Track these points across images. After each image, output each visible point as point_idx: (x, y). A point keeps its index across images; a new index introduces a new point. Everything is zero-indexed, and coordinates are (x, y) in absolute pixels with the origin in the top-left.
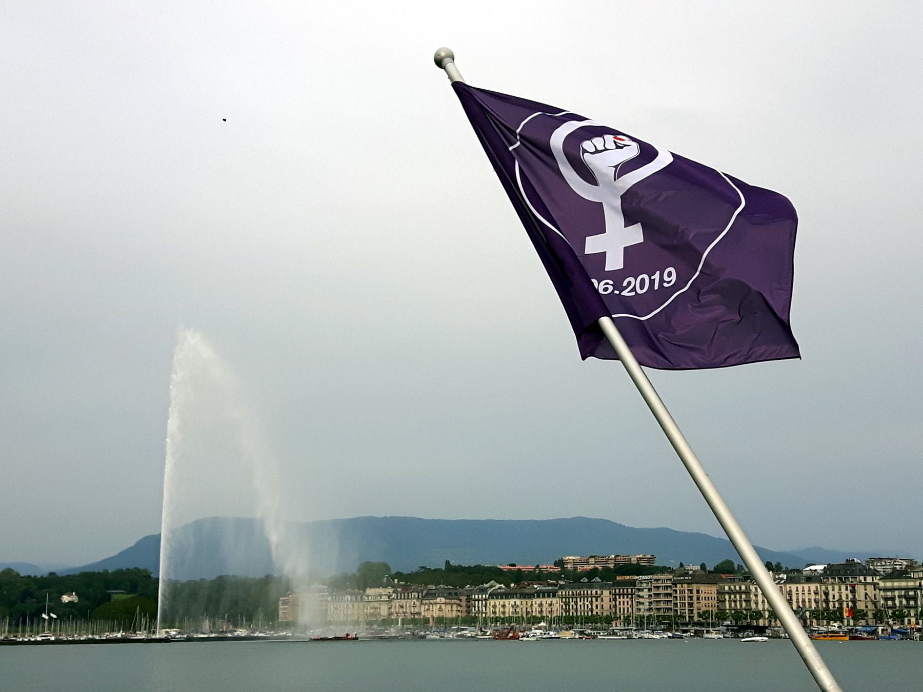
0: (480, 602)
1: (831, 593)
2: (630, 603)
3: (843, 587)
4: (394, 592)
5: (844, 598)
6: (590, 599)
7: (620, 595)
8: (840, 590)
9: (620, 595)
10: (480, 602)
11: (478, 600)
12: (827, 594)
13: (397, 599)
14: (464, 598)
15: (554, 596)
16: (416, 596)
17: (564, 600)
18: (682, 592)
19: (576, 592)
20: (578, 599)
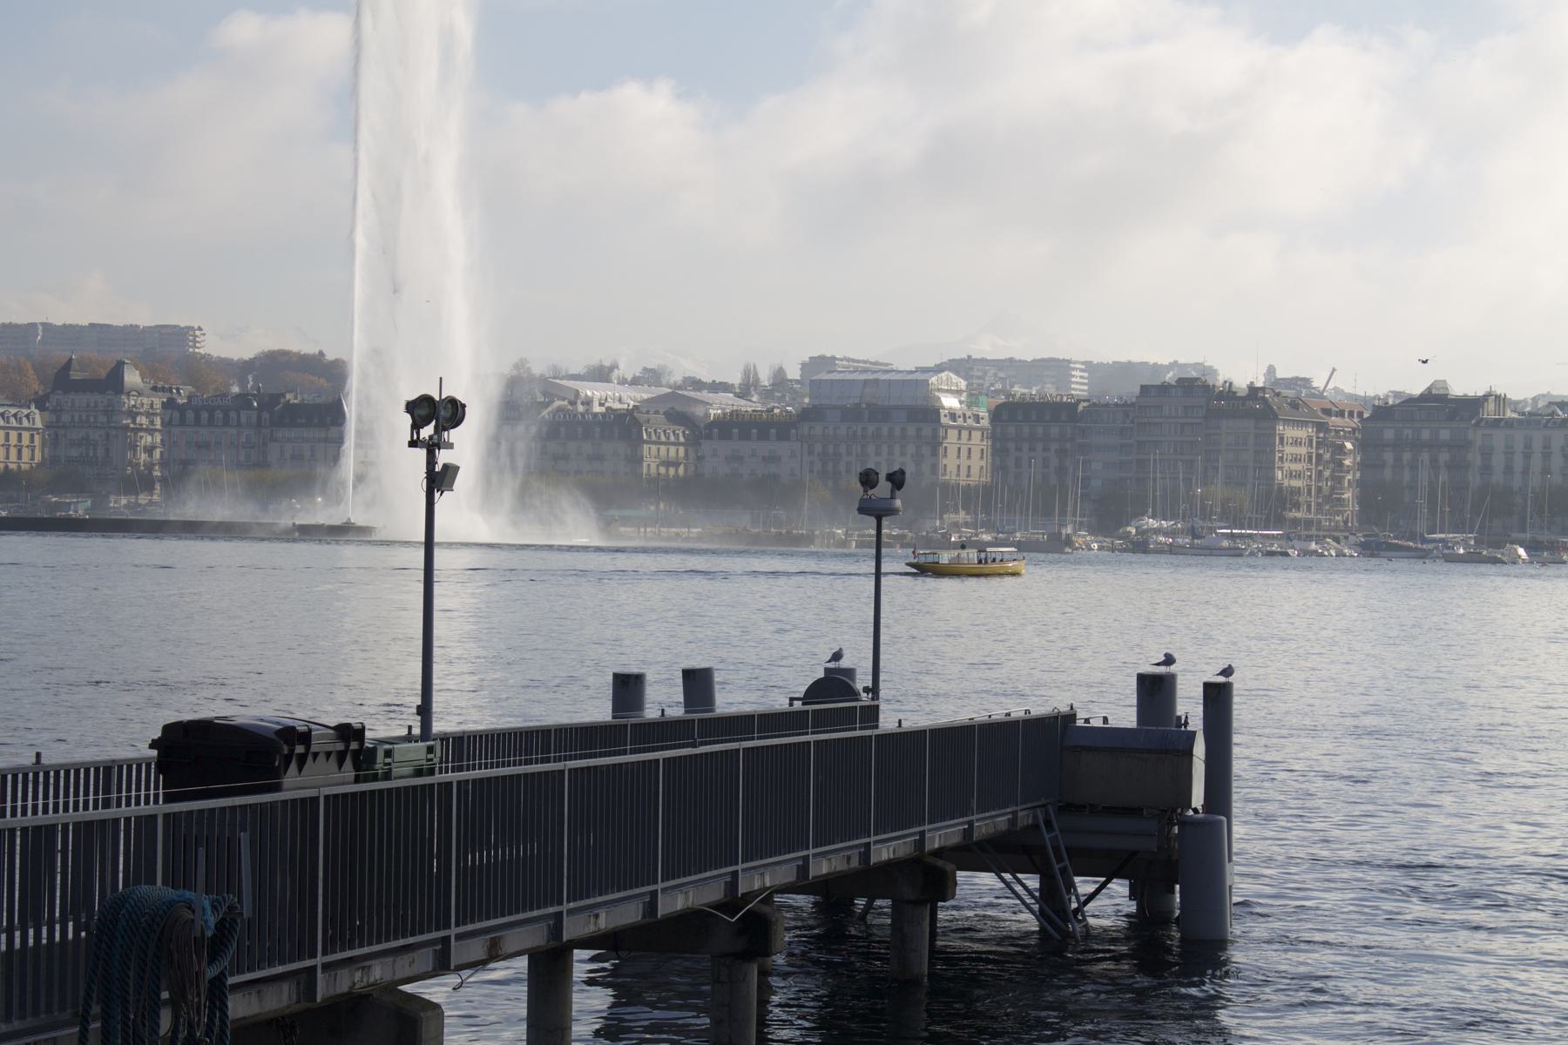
4: (170, 405)
13: (183, 422)
16: (254, 420)
17: (818, 448)
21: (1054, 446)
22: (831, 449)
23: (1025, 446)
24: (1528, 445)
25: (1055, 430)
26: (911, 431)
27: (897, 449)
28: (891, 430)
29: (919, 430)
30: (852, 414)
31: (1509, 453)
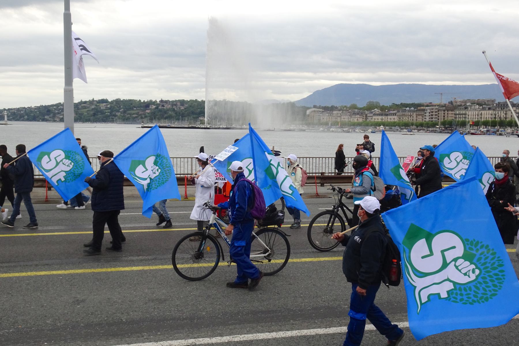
1: (497, 115)
2: (422, 118)
3: (502, 112)
5: (502, 117)
7: (418, 115)
8: (501, 113)
9: (418, 115)
12: (495, 115)
14: (364, 115)
15: (395, 115)
18: (441, 114)
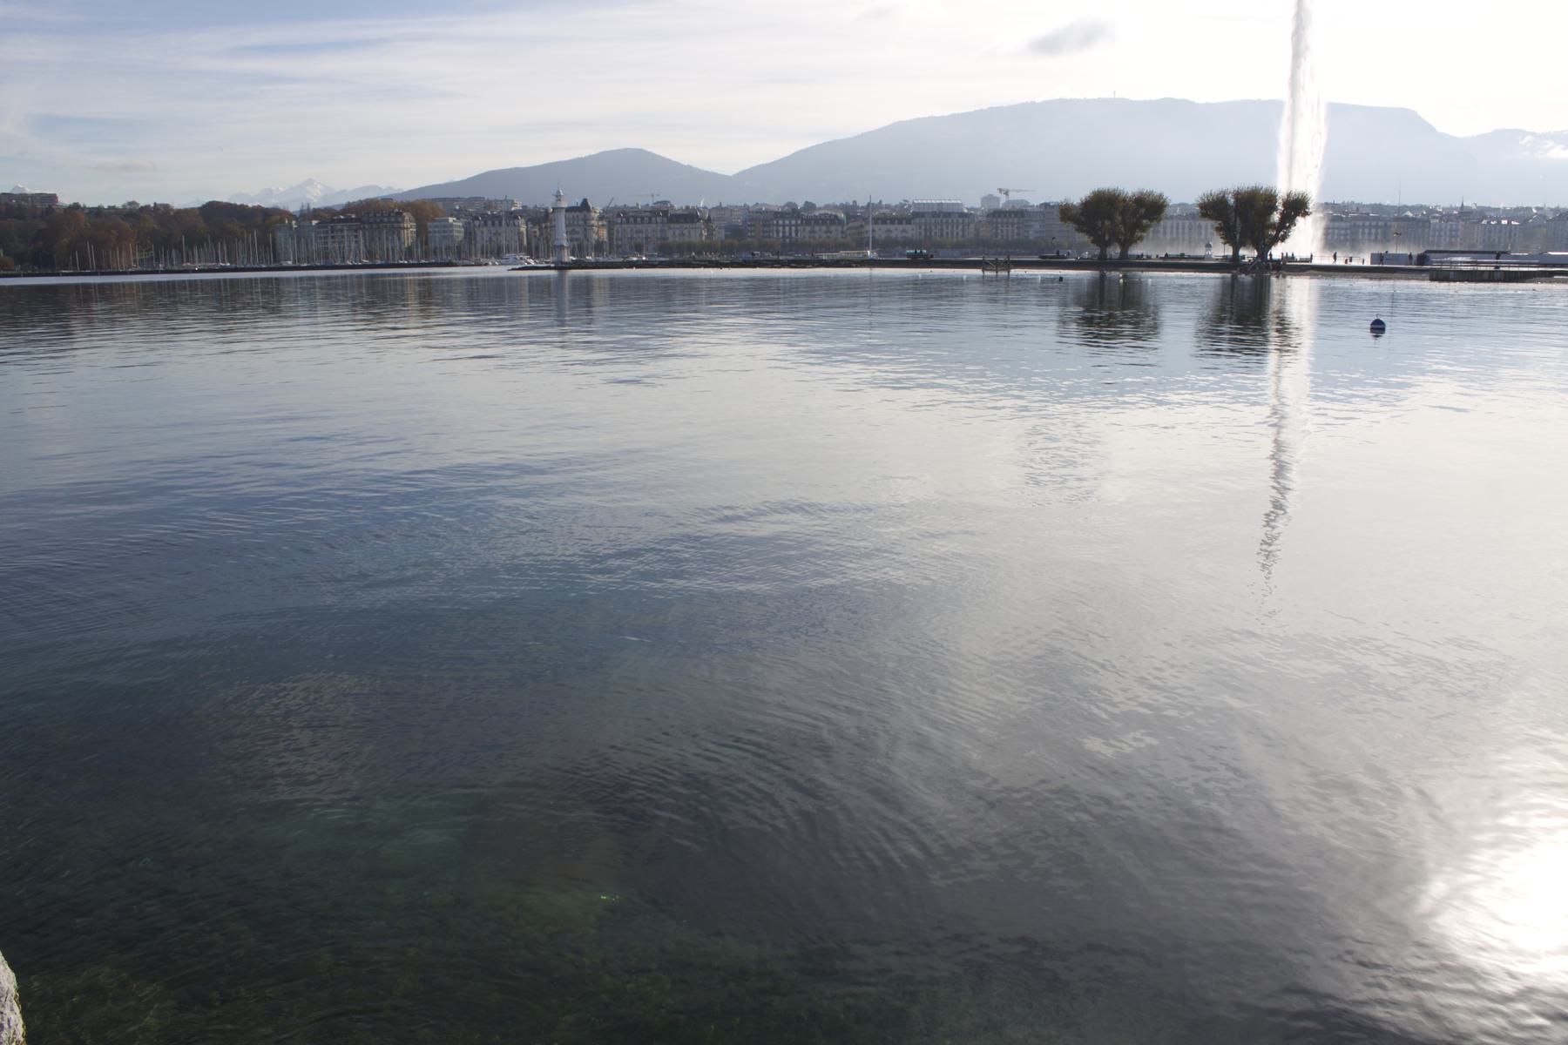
0: (787, 228)
6: (961, 227)
10: (787, 228)
11: (784, 226)
19: (942, 221)
20: (945, 227)
21: (1016, 226)
22: (928, 227)
23: (1005, 226)
24: (1178, 225)
25: (1016, 220)
26: (961, 220)
27: (955, 227)
28: (952, 221)
29: (964, 221)
30: (934, 215)
31: (1172, 228)
